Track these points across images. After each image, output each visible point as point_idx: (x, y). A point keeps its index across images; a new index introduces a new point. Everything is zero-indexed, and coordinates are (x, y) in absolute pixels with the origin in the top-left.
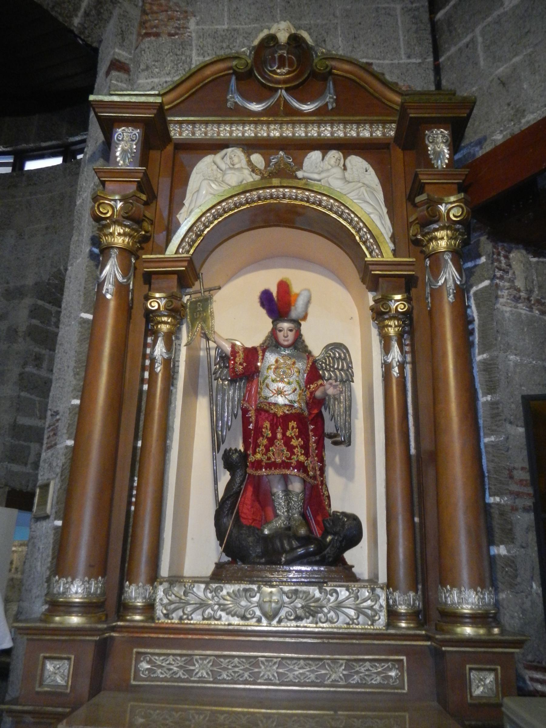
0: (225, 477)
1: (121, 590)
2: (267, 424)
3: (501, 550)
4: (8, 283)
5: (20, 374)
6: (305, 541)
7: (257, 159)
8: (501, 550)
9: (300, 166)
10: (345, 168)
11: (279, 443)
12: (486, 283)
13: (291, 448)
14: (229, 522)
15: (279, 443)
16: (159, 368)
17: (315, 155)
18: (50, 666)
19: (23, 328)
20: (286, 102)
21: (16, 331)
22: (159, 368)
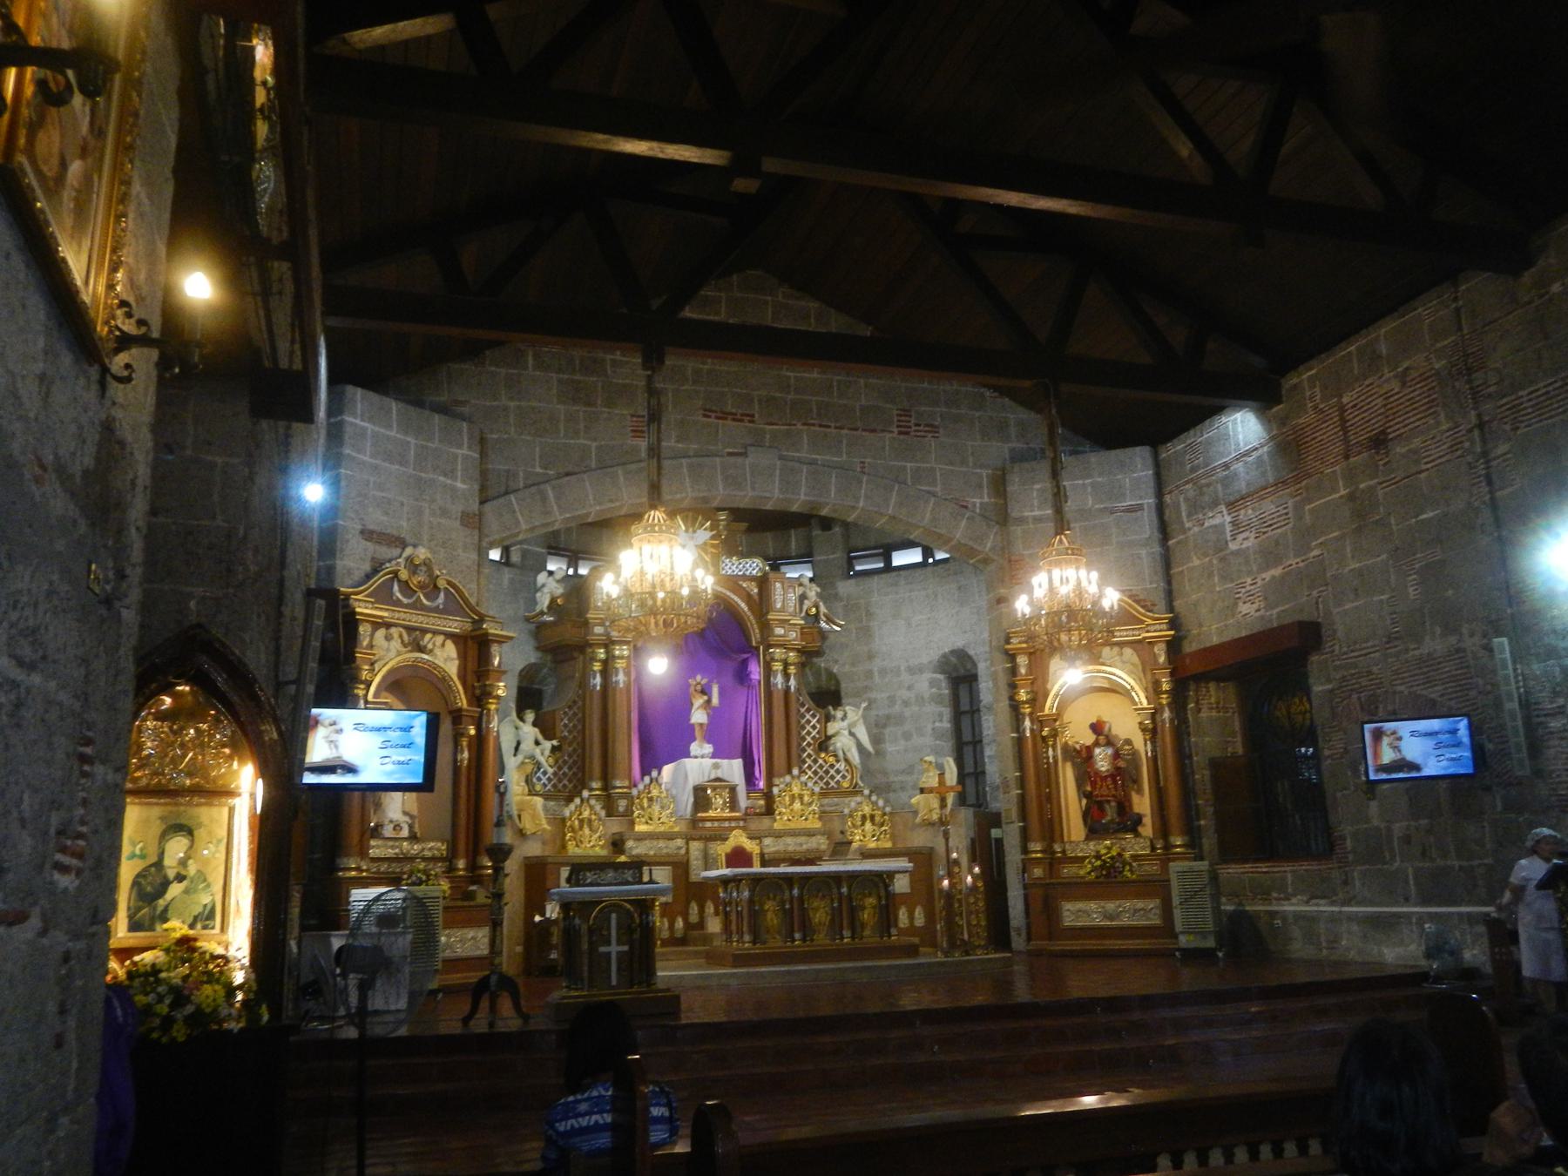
0: (1084, 801)
1: (1052, 847)
2: (1098, 779)
3: (1202, 822)
4: (907, 661)
5: (933, 729)
6: (1119, 824)
8: (1202, 822)
10: (1122, 654)
11: (1104, 788)
12: (1192, 705)
13: (1109, 789)
14: (1089, 821)
15: (1104, 788)
16: (1051, 760)
18: (1035, 870)
19: (926, 696)
21: (922, 698)
22: (1051, 760)
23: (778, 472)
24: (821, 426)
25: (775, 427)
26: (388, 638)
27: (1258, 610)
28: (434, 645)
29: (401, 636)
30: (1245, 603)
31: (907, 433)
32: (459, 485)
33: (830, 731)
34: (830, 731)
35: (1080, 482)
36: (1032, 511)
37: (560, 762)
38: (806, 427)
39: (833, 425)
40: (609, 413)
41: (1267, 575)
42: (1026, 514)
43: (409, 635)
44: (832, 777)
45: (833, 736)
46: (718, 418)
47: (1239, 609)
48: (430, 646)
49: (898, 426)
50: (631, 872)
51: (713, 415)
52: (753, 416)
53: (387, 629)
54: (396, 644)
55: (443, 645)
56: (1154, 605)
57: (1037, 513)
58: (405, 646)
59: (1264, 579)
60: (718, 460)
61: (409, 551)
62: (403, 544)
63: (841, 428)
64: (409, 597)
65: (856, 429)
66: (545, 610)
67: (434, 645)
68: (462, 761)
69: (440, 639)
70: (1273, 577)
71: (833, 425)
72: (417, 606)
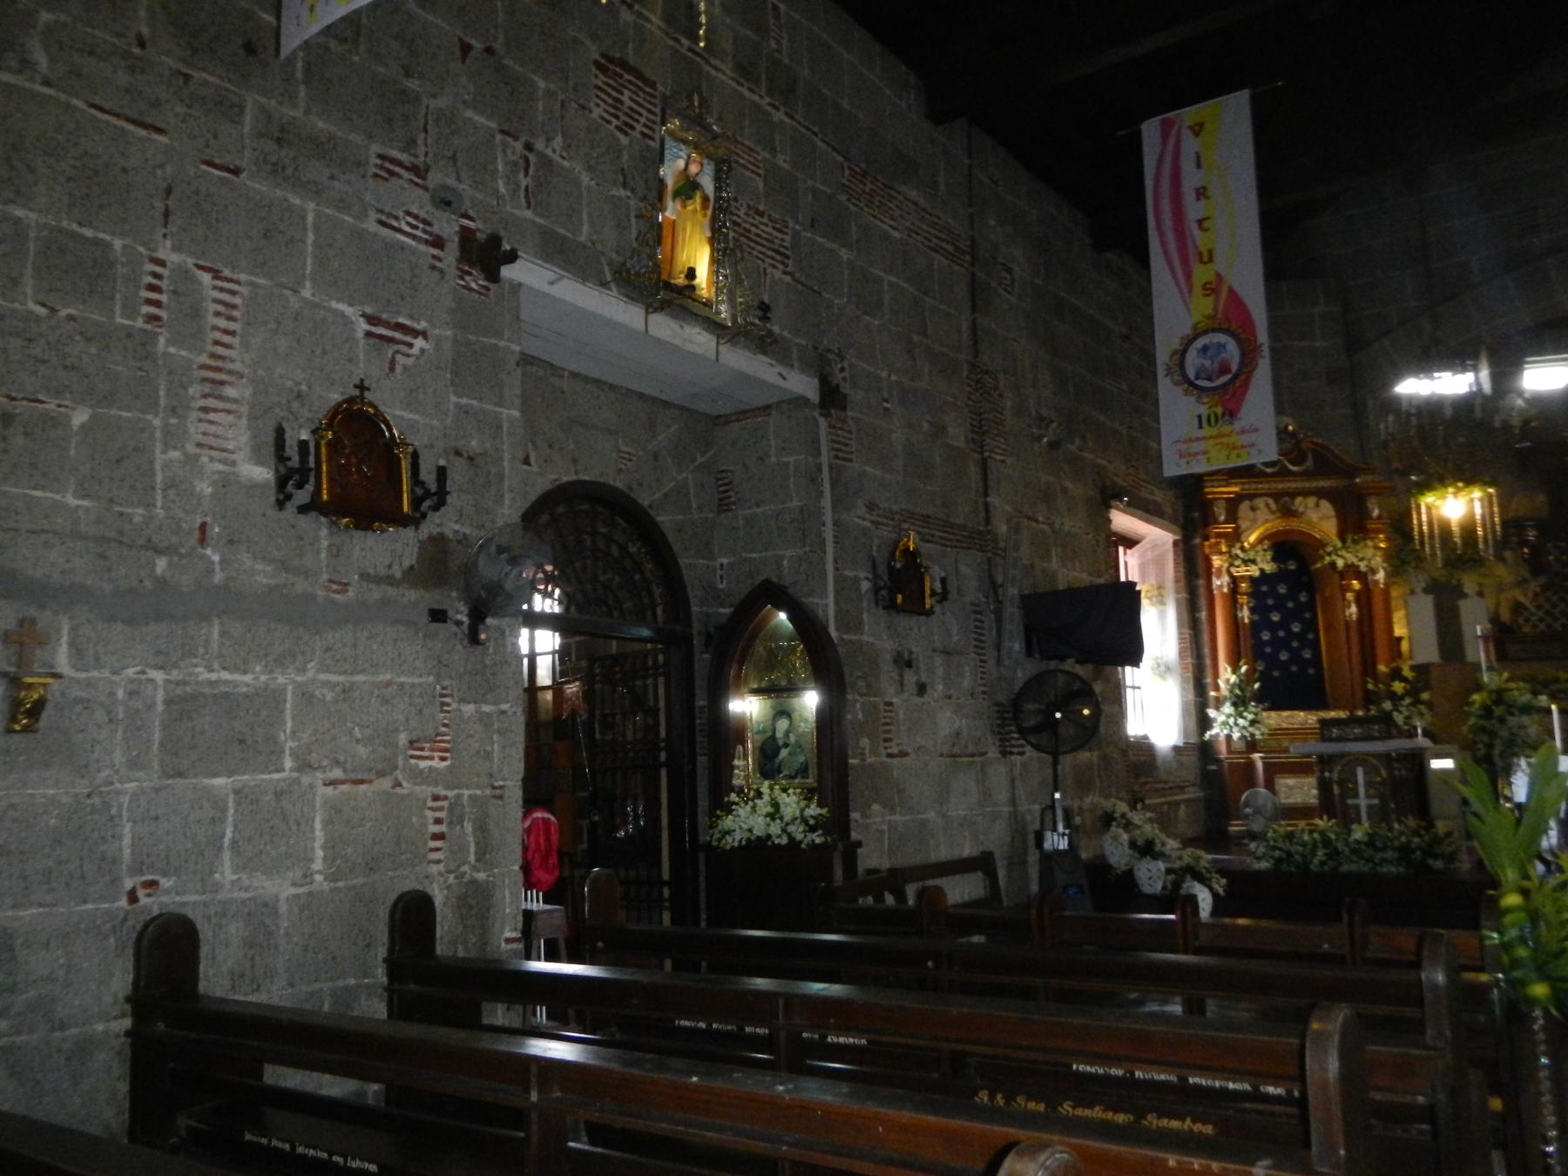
26: (1253, 509)
28: (1306, 507)
29: (1267, 505)
37: (1555, 598)
43: (1277, 502)
48: (1301, 509)
54: (1263, 514)
55: (1317, 505)
58: (1273, 513)
67: (1306, 507)
69: (1311, 501)
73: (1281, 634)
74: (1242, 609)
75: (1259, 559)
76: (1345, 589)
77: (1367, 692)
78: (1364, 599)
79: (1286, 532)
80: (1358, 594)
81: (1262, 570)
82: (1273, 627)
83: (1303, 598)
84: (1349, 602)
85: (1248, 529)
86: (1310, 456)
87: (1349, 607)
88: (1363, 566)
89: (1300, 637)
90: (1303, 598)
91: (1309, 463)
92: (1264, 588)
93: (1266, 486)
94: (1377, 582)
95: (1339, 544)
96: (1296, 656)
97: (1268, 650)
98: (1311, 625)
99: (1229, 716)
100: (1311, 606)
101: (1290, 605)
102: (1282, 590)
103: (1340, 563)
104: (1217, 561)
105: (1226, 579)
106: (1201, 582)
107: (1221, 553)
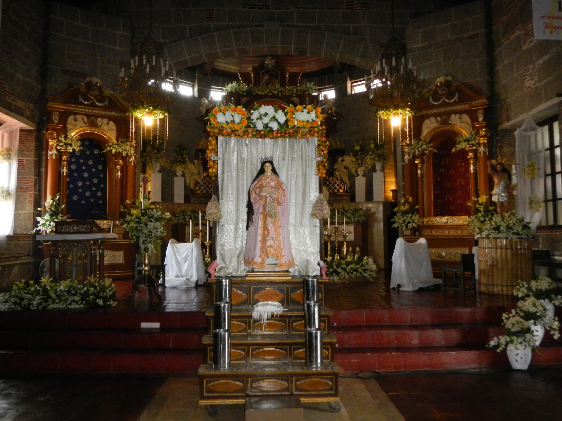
7: (439, 118)
9: (449, 120)
10: (461, 118)
16: (419, 176)
17: (453, 116)
20: (446, 102)
23: (280, 33)
24: (303, 8)
25: (278, 11)
26: (75, 120)
27: (535, 84)
28: (102, 124)
29: (83, 119)
30: (528, 81)
31: (352, 9)
32: (118, 48)
33: (335, 167)
34: (335, 167)
35: (444, 25)
36: (417, 44)
38: (296, 10)
39: (310, 7)
40: (195, 10)
41: (540, 62)
42: (415, 46)
43: (88, 119)
44: (336, 188)
45: (336, 169)
46: (249, 8)
47: (525, 85)
48: (100, 124)
49: (347, 5)
50: (86, 226)
51: (248, 7)
52: (268, 6)
53: (75, 116)
54: (80, 123)
55: (108, 123)
56: (481, 90)
57: (420, 45)
58: (86, 123)
59: (539, 64)
60: (249, 29)
61: (88, 79)
62: (86, 76)
63: (316, 8)
64: (88, 101)
65: (323, 8)
66: (204, 115)
68: (118, 176)
69: (105, 121)
70: (544, 62)
71: (310, 7)
72: (93, 105)
73: (88, 183)
74: (63, 168)
75: (73, 144)
76: (116, 164)
77: (121, 212)
78: (124, 169)
79: (91, 134)
80: (122, 167)
81: (74, 150)
82: (84, 180)
83: (100, 167)
84: (118, 170)
85: (71, 129)
86: (107, 99)
87: (117, 173)
88: (124, 154)
89: (97, 185)
90: (100, 167)
91: (106, 103)
92: (82, 161)
93: (83, 110)
94: (131, 162)
95: (115, 142)
96: (94, 194)
97: (80, 190)
98: (103, 181)
99: (47, 221)
100: (104, 171)
101: (94, 170)
102: (90, 162)
103: (114, 151)
104: (51, 143)
105: (54, 152)
106: (44, 153)
107: (53, 139)
